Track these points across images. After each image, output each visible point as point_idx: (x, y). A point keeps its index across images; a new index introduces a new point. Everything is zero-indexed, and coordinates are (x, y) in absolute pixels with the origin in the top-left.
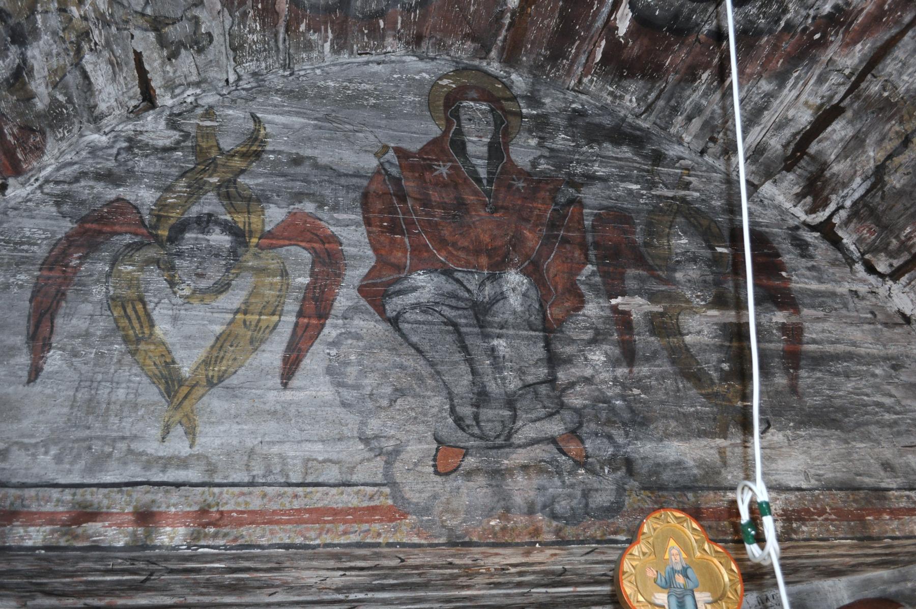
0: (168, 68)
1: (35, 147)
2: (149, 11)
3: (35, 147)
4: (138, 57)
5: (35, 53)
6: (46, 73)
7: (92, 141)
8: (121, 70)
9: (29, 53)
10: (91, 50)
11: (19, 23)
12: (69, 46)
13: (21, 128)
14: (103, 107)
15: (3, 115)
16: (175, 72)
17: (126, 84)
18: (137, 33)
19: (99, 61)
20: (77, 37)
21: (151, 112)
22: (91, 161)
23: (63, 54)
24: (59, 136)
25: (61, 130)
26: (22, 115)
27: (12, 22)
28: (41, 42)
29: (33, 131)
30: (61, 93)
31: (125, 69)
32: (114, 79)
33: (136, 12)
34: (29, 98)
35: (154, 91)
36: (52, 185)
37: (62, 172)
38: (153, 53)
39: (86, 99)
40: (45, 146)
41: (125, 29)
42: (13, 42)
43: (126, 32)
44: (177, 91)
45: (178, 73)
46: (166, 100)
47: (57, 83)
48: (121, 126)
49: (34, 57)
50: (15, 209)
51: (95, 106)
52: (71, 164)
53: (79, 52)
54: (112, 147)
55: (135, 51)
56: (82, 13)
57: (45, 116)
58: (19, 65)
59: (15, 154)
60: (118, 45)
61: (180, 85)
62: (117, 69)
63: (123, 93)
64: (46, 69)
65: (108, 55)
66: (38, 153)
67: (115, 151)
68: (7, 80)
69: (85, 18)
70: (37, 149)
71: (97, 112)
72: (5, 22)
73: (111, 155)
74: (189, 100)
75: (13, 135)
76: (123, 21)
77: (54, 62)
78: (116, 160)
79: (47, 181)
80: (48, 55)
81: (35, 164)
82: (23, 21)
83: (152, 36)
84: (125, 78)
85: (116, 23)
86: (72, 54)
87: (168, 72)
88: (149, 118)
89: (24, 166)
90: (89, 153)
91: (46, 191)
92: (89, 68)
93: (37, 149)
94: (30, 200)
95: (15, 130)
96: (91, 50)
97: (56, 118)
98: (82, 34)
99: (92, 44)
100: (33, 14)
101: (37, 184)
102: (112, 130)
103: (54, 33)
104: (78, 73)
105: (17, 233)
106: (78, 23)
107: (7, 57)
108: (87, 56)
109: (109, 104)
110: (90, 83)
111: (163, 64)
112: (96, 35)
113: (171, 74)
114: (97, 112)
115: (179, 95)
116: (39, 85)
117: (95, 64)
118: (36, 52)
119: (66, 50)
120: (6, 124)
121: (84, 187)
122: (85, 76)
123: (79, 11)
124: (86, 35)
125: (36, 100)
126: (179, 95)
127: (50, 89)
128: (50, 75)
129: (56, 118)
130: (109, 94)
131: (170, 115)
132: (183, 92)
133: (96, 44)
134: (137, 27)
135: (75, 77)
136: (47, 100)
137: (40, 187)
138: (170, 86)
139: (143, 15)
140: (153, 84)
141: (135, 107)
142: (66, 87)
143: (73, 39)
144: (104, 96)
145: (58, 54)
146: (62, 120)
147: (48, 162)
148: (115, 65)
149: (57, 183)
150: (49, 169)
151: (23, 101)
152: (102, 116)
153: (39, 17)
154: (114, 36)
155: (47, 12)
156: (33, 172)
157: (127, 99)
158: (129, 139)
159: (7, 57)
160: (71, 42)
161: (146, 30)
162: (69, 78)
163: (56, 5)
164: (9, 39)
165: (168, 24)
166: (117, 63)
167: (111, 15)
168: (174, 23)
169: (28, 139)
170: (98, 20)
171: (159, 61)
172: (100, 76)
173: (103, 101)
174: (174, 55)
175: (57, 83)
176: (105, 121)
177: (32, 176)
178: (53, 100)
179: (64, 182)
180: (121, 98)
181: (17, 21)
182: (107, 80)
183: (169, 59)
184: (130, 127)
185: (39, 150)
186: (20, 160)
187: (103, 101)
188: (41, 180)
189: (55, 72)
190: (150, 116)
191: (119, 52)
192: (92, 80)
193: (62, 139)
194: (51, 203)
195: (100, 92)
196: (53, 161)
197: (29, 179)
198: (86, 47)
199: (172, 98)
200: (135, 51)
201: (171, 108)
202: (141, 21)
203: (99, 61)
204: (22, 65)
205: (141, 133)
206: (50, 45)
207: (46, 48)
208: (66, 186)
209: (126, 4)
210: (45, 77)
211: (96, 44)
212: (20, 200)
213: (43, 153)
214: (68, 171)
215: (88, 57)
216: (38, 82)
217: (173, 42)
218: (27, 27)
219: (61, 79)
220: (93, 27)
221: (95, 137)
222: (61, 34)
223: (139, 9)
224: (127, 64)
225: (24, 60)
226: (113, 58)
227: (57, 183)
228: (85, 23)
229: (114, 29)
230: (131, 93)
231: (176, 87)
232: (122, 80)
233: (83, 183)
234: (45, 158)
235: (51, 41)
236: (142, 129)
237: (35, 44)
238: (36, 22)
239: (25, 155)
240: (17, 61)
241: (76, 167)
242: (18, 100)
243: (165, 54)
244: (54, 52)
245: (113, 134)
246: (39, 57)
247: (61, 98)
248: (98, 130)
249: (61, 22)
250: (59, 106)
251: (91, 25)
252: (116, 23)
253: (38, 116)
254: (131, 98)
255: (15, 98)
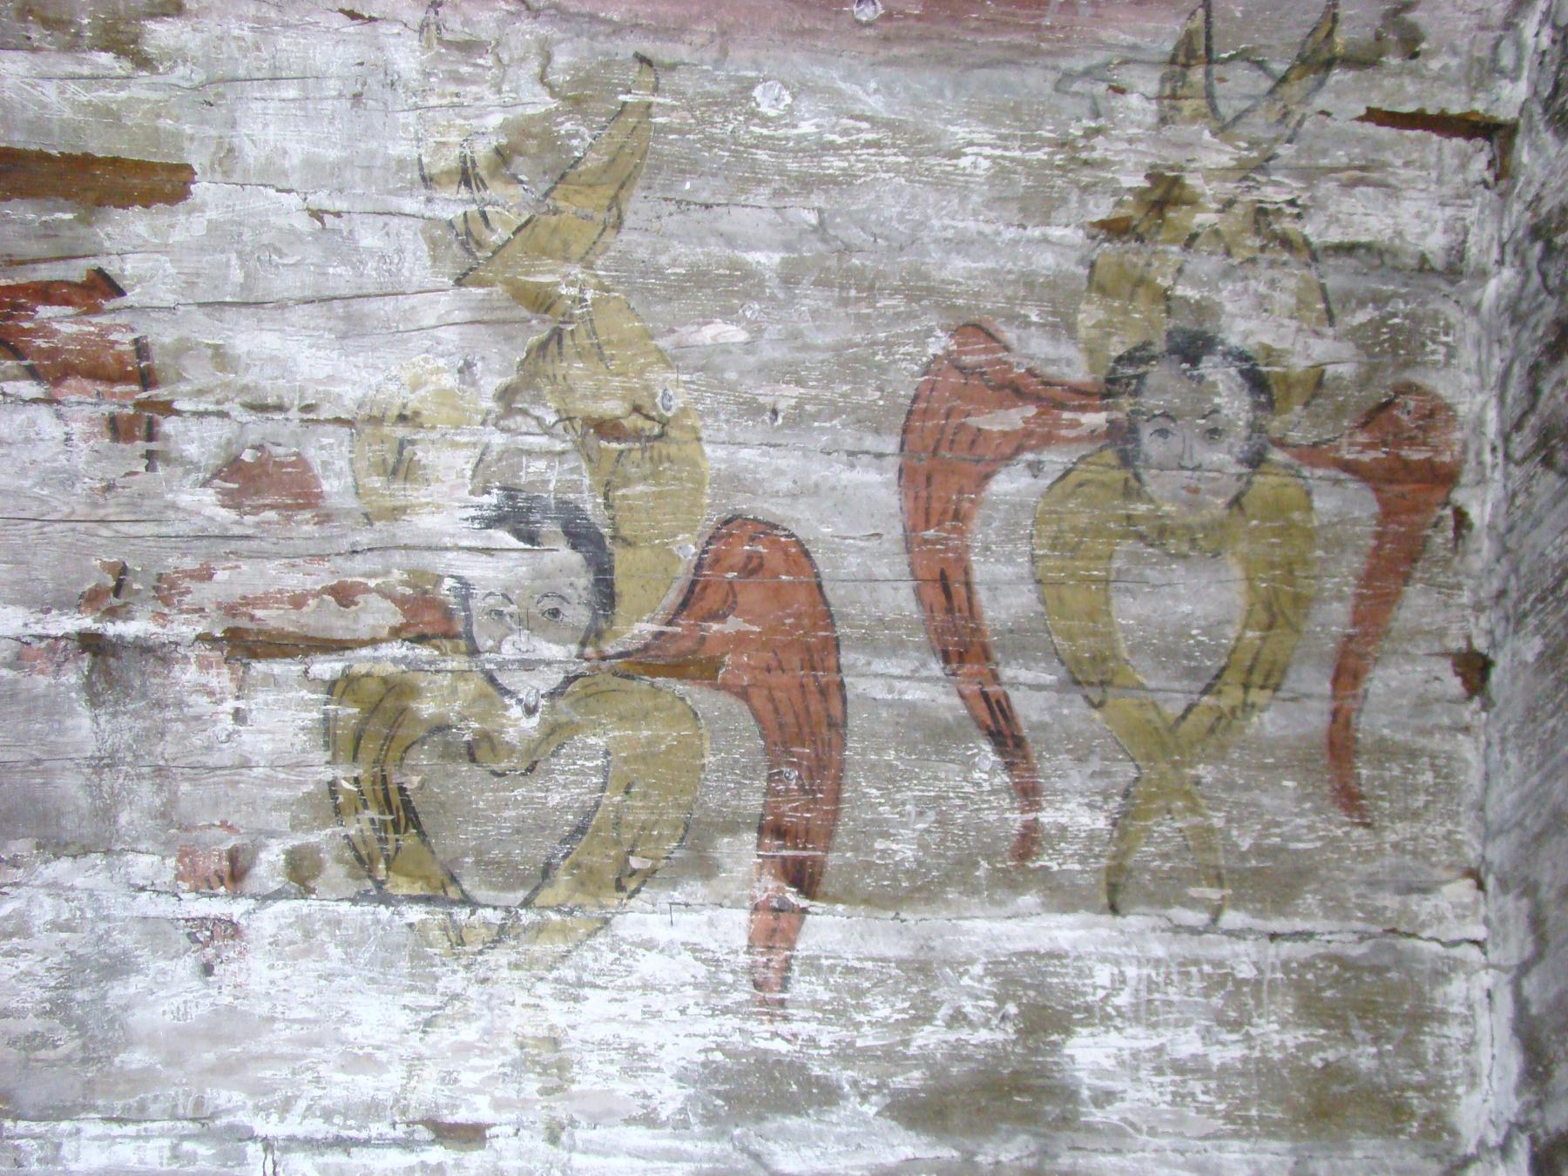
0: (1435, 65)
1: (1423, 417)
2: (1279, 67)
3: (1423, 417)
4: (1375, 116)
5: (1242, 328)
6: (1294, 324)
7: (1499, 297)
8: (1383, 166)
9: (1234, 340)
10: (1299, 216)
11: (1170, 334)
12: (1268, 255)
13: (1363, 426)
14: (1435, 243)
15: (1315, 445)
16: (1455, 52)
17: (1422, 167)
18: (1320, 102)
19: (1332, 209)
20: (1257, 233)
21: (1518, 141)
22: (1525, 335)
23: (1275, 273)
24: (1440, 357)
25: (1430, 347)
26: (1340, 411)
27: (1160, 346)
28: (1229, 307)
29: (1389, 404)
30: (1354, 311)
31: (1388, 156)
32: (1392, 191)
33: (1271, 92)
34: (1317, 383)
35: (1475, 113)
36: (1516, 438)
37: (1509, 400)
38: (1380, 86)
39: (1395, 269)
40: (1437, 397)
41: (1300, 123)
42: (1194, 361)
43: (1306, 124)
44: (1507, 60)
45: (1463, 44)
46: (1510, 97)
47: (1328, 311)
48: (1506, 225)
49: (1246, 335)
50: (1510, 529)
51: (1423, 258)
52: (1505, 376)
53: (1286, 242)
54: (1528, 274)
55: (1361, 119)
56: (1214, 206)
57: (1374, 368)
58: (1242, 373)
59: (1406, 464)
60: (1324, 153)
61: (1495, 47)
62: (1375, 175)
63: (1439, 181)
64: (1286, 322)
65: (1332, 185)
66: (1441, 416)
67: (1536, 278)
68: (1257, 406)
69: (1228, 204)
70: (1431, 414)
71: (1438, 262)
72: (1153, 358)
73: (1537, 293)
74: (1545, 42)
75: (1366, 447)
76: (1280, 122)
77: (1284, 299)
78: (1550, 293)
79: (1506, 438)
80: (1262, 305)
81: (1458, 435)
82: (1171, 324)
83: (1337, 75)
84: (1407, 164)
85: (1276, 140)
86: (1286, 256)
87: (1445, 68)
88: (1525, 157)
89: (1447, 458)
90: (1512, 323)
91: (1518, 453)
92: (1335, 236)
93: (1431, 414)
94: (1514, 495)
95: (1362, 438)
96: (1299, 216)
97: (1395, 345)
98: (1256, 222)
99: (1289, 210)
100: (1168, 298)
101: (1500, 454)
102: (1502, 246)
103: (1227, 274)
104: (1331, 261)
105: (1542, 570)
106: (1228, 224)
107: (1214, 384)
108: (1308, 230)
109: (1440, 226)
110: (1368, 247)
111: (1415, 74)
112: (1273, 195)
113: (1454, 62)
114: (1438, 262)
115: (1519, 59)
116: (1307, 347)
117: (1334, 220)
118: (1241, 325)
119: (1272, 264)
120: (1337, 449)
121: (1552, 395)
122: (1349, 249)
123: (1208, 211)
124: (1261, 213)
125: (1330, 370)
126: (1519, 59)
127: (1330, 331)
128: (1301, 319)
129: (1396, 345)
130: (1418, 215)
131: (1546, 110)
132: (1519, 46)
133: (1292, 203)
134: (1305, 100)
135: (1337, 269)
136: (1347, 349)
137: (1507, 456)
138: (1487, 71)
139: (1283, 80)
140: (1455, 110)
141: (1490, 164)
142: (1346, 297)
143: (1258, 242)
144: (1412, 229)
145: (1272, 283)
146: (1411, 333)
147: (1476, 408)
148: (1365, 175)
149: (1518, 427)
150: (1491, 415)
151: (1314, 396)
152: (1458, 253)
153: (1180, 291)
154: (1299, 155)
155: (1180, 271)
156: (1473, 447)
157: (1459, 178)
158: (1535, 232)
159: (1214, 384)
160: (1263, 249)
161: (1321, 84)
162: (1333, 282)
163: (1175, 248)
164: (1185, 366)
165: (1330, 34)
166: (1362, 168)
167: (1253, 144)
168: (1335, 19)
169: (1396, 422)
170: (1245, 178)
171: (1407, 81)
172: (1365, 217)
173: (1424, 235)
174: (1411, 45)
175: (1328, 311)
176: (1473, 251)
177: (1479, 454)
178: (1354, 334)
179: (1524, 414)
180: (1446, 191)
181: (1163, 335)
182: (1385, 208)
183: (1414, 55)
184: (1517, 207)
185: (1436, 413)
186: (1428, 460)
187: (1424, 235)
188: (1499, 443)
189: (1302, 303)
190: (1524, 154)
191: (1340, 156)
192: (1364, 239)
193: (1451, 352)
194: (1540, 470)
195: (1399, 234)
196: (1480, 398)
197: (1480, 463)
198: (1286, 225)
199: (1515, 79)
200: (1361, 119)
201: (1536, 93)
202: (1294, 90)
203: (1332, 209)
204: (1246, 366)
205: (1538, 198)
206: (1246, 290)
207: (1246, 302)
208: (1533, 420)
209: (1246, 104)
210: (1299, 330)
211: (1292, 203)
212: (1503, 508)
213: (1448, 407)
214: (1515, 388)
215: (1313, 230)
216: (1298, 348)
217: (1378, 38)
218: (1185, 322)
219: (1325, 299)
220: (1255, 195)
221: (1492, 287)
222: (1236, 261)
223: (1267, 84)
224: (1379, 146)
225: (1242, 356)
226: (1344, 176)
227: (1518, 427)
228: (1238, 209)
229: (1285, 151)
230: (1451, 162)
231: (1495, 59)
232: (1406, 173)
233: (1546, 388)
234: (1462, 409)
235: (1239, 286)
236: (1533, 190)
237: (1224, 320)
238: (1185, 300)
239: (1424, 444)
240: (1233, 371)
241: (1516, 369)
242: (1306, 405)
243: (1393, 61)
244: (1262, 289)
245: (1509, 249)
246: (1253, 324)
247: (1361, 317)
248: (1483, 275)
249: (1211, 253)
250: (1377, 331)
251: (1248, 198)
252: (1276, 140)
253: (1363, 382)
254: (1463, 167)
255: (1298, 408)
